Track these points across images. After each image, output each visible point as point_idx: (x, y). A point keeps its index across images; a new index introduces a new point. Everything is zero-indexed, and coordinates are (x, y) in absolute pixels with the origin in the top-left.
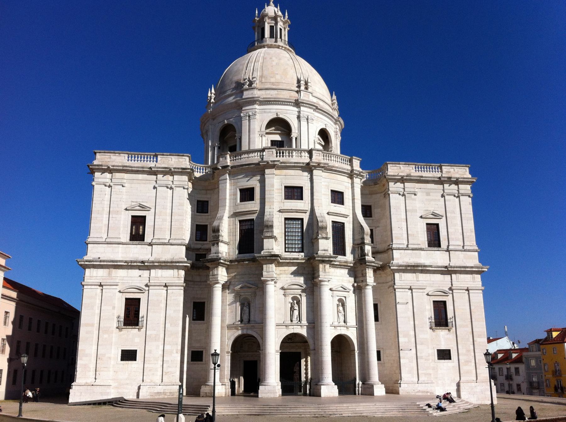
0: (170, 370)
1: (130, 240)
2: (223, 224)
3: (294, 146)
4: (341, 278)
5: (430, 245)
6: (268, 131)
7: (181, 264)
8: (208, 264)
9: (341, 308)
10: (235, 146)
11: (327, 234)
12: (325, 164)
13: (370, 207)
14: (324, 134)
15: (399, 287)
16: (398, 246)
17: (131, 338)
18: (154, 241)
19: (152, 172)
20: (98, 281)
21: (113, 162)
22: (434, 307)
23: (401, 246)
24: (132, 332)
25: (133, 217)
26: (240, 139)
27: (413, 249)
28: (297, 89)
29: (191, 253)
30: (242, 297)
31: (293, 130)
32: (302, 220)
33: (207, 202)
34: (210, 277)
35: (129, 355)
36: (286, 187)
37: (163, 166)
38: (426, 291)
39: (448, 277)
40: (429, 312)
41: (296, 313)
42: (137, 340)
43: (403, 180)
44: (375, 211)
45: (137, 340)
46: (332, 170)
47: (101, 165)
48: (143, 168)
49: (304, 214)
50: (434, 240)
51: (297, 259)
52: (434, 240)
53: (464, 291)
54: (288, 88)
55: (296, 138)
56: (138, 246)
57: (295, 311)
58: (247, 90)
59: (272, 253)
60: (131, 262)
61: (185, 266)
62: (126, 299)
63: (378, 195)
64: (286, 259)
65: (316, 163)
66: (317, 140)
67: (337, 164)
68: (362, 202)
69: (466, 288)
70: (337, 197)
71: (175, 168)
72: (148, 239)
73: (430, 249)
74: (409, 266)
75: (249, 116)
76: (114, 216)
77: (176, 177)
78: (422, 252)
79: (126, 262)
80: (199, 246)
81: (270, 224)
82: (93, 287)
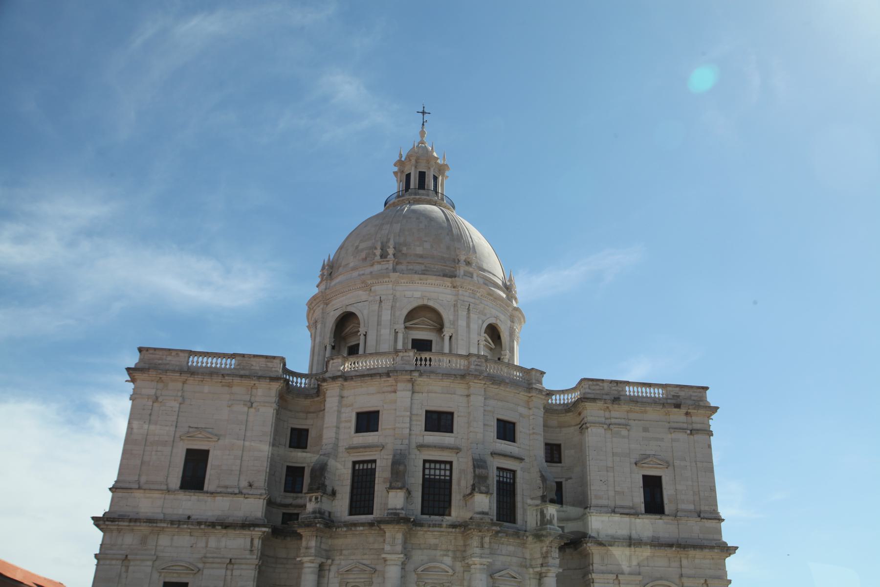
3: (447, 350)
6: (408, 324)
7: (257, 529)
8: (299, 531)
10: (358, 345)
11: (488, 487)
13: (558, 446)
14: (493, 332)
18: (219, 490)
21: (166, 364)
26: (365, 335)
32: (451, 463)
33: (307, 431)
34: (303, 550)
36: (427, 412)
44: (566, 453)
55: (451, 337)
58: (379, 263)
59: (401, 515)
61: (264, 532)
63: (572, 429)
68: (544, 439)
70: (506, 430)
72: (210, 483)
76: (159, 448)
80: (289, 501)
81: (401, 468)
82: (114, 562)
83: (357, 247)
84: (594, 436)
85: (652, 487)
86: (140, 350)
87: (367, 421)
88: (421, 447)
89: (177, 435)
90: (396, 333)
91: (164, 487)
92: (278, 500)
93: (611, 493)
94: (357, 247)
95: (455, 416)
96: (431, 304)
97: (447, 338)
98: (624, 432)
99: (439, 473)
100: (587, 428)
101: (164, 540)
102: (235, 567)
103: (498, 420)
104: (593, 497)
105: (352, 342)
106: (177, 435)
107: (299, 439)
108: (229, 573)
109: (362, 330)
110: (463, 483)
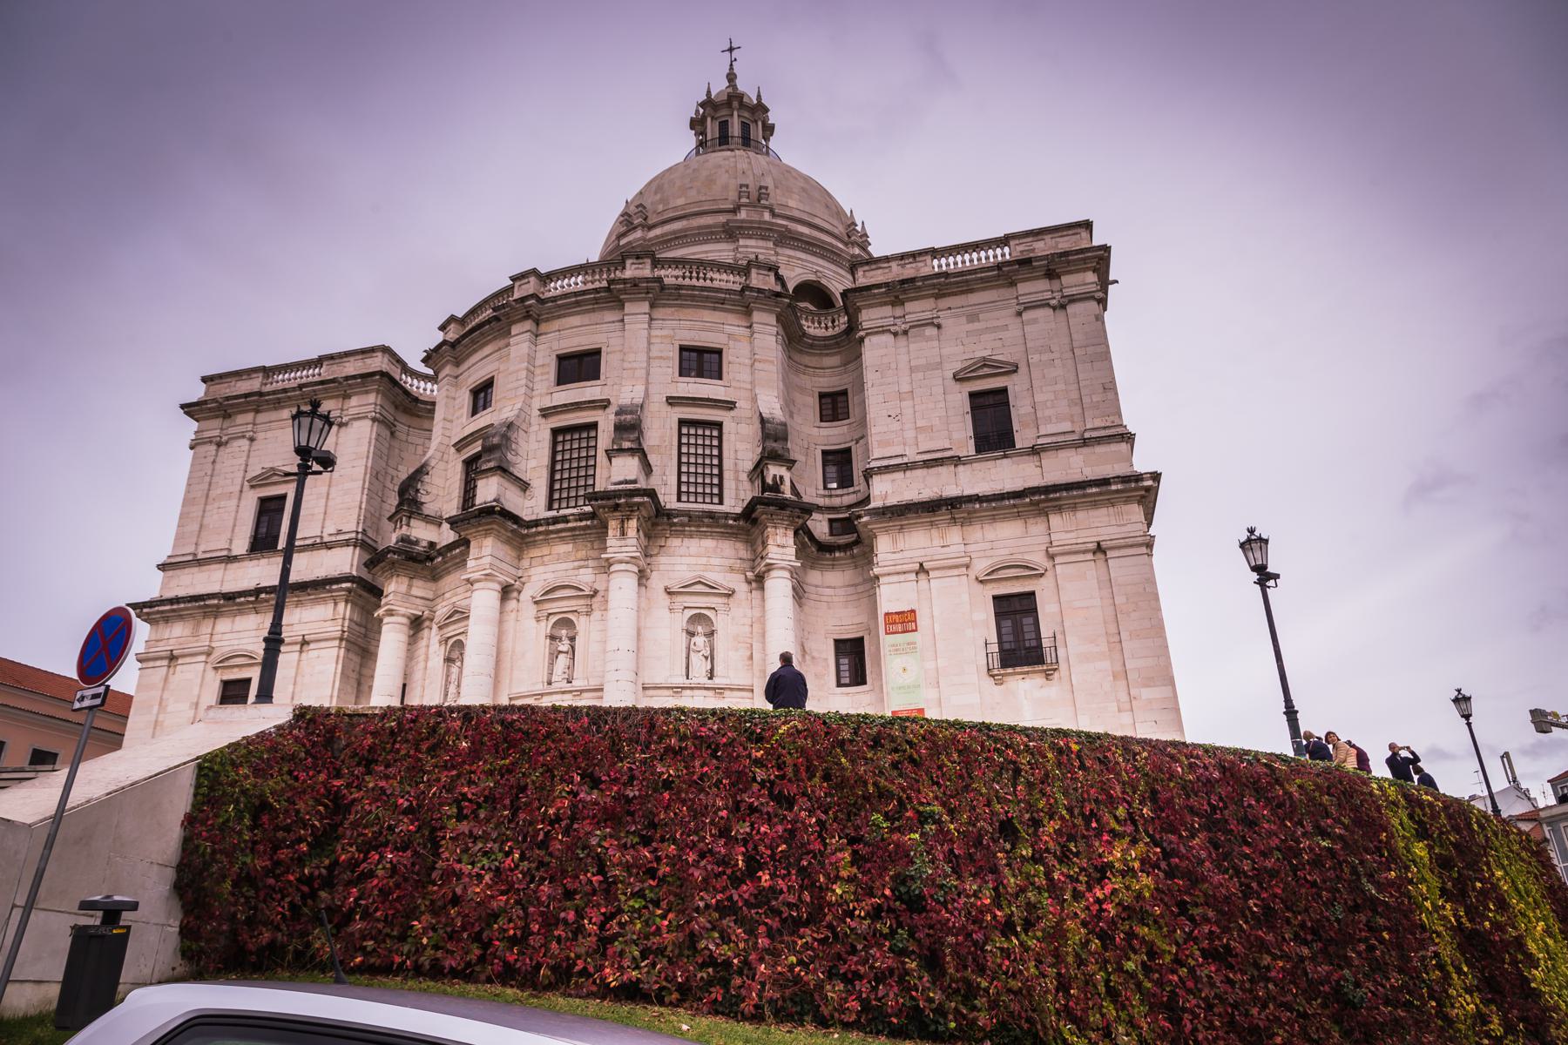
2: (426, 478)
4: (704, 560)
5: (979, 450)
9: (700, 640)
15: (886, 570)
16: (885, 463)
22: (999, 615)
27: (928, 464)
30: (451, 642)
39: (1037, 527)
40: (983, 626)
41: (562, 661)
46: (680, 297)
48: (285, 391)
49: (600, 412)
53: (1090, 556)
56: (263, 561)
57: (561, 656)
61: (349, 590)
69: (1093, 546)
70: (701, 361)
71: (347, 378)
76: (223, 504)
77: (354, 401)
78: (961, 468)
82: (158, 663)
84: (875, 350)
86: (204, 380)
88: (546, 413)
93: (910, 434)
98: (931, 331)
100: (862, 340)
101: (223, 625)
102: (312, 646)
103: (683, 349)
104: (875, 444)
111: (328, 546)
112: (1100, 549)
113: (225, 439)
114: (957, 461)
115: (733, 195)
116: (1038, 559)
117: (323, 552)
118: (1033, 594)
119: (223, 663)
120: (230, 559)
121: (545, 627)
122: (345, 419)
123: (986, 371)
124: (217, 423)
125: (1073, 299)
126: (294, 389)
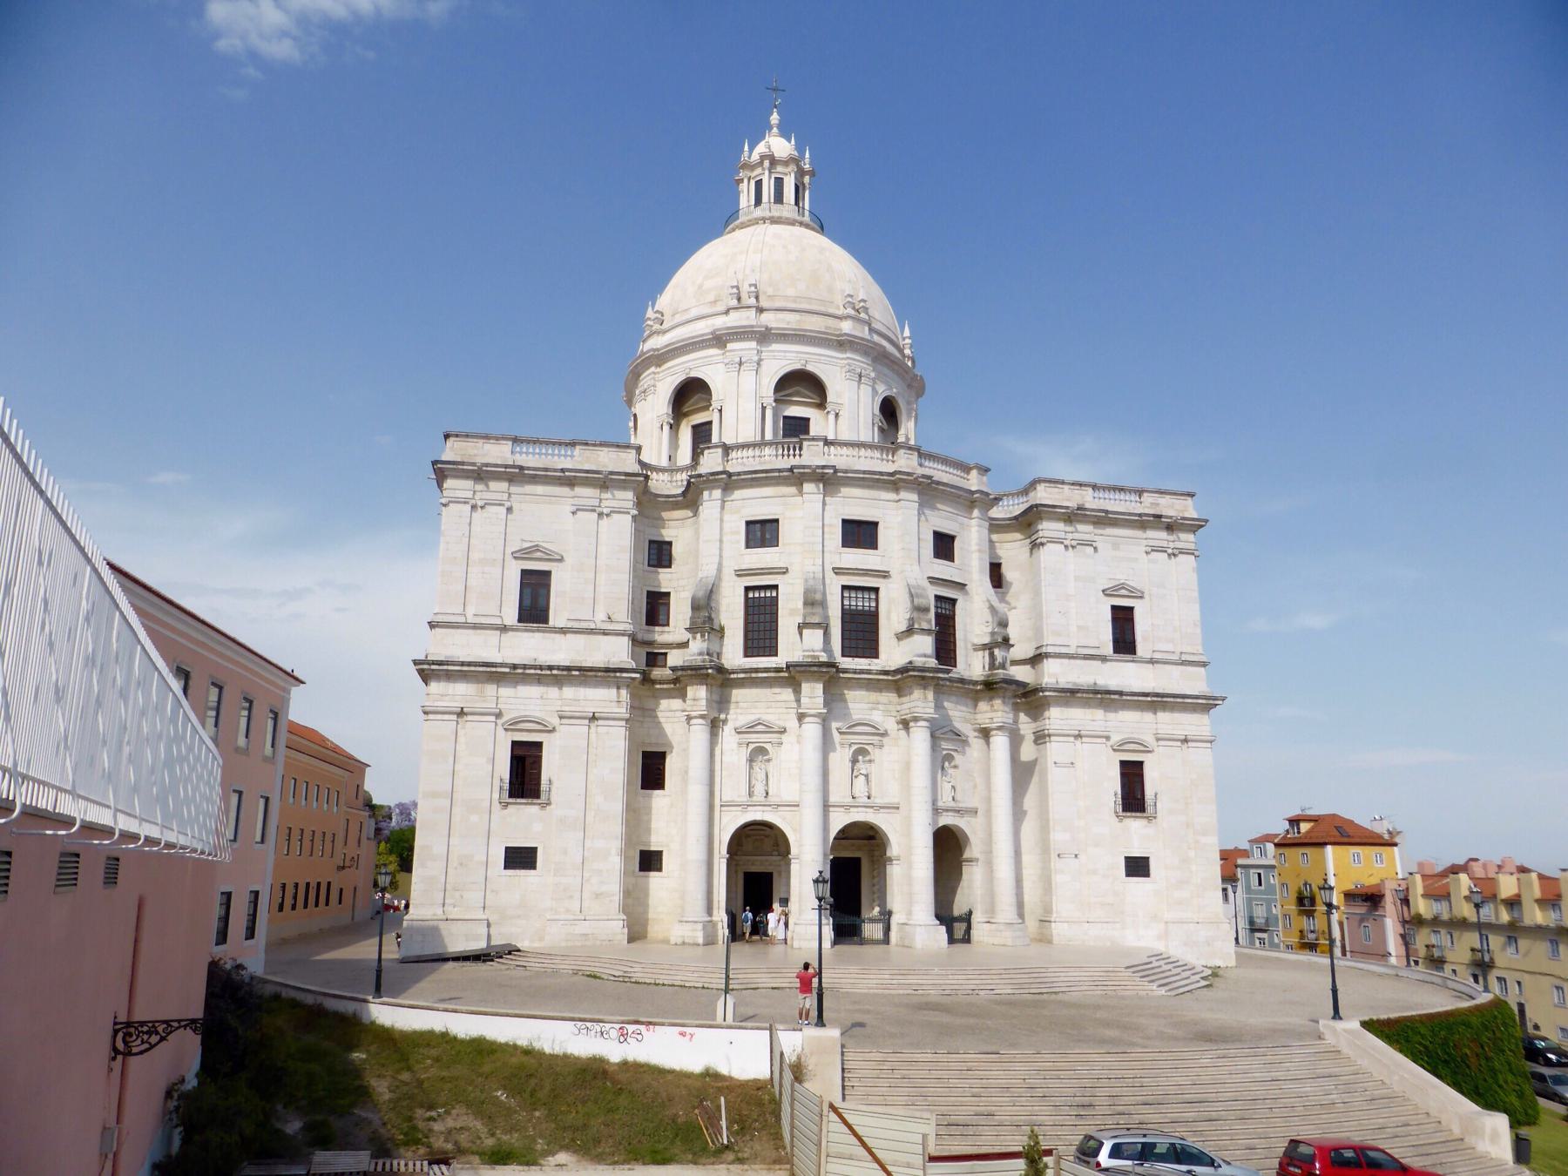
0: (604, 888)
1: (520, 620)
5: (1117, 650)
10: (710, 423)
12: (924, 476)
14: (889, 411)
16: (1057, 650)
17: (523, 823)
18: (570, 625)
19: (568, 480)
20: (456, 705)
22: (1123, 775)
23: (1063, 650)
24: (524, 812)
25: (524, 573)
28: (841, 312)
29: (637, 649)
30: (752, 746)
31: (831, 397)
32: (876, 590)
35: (521, 858)
36: (845, 522)
37: (586, 467)
38: (1112, 742)
39: (1148, 716)
40: (1113, 783)
42: (537, 827)
43: (1073, 516)
45: (537, 827)
47: (463, 463)
48: (546, 470)
50: (1124, 641)
51: (869, 672)
52: (1124, 641)
54: (823, 309)
55: (837, 415)
56: (537, 635)
60: (525, 667)
62: (514, 743)
64: (845, 671)
65: (908, 474)
66: (877, 420)
67: (945, 478)
70: (944, 545)
72: (557, 617)
73: (1118, 656)
74: (1078, 691)
75: (741, 364)
79: (515, 667)
81: (818, 597)
82: (446, 717)
83: (700, 287)
85: (1123, 620)
87: (762, 532)
88: (838, 571)
89: (509, 551)
90: (764, 408)
91: (498, 621)
92: (639, 636)
94: (700, 287)
95: (880, 527)
96: (810, 368)
97: (832, 417)
99: (861, 603)
101: (506, 692)
102: (600, 722)
105: (699, 418)
106: (509, 551)
107: (660, 554)
108: (593, 729)
109: (715, 404)
110: (894, 617)
111: (605, 633)
112: (1186, 741)
113: (480, 503)
114: (1104, 659)
115: (840, 301)
116: (1149, 739)
117: (601, 637)
118: (1141, 764)
119: (512, 726)
120: (504, 629)
121: (847, 753)
122: (606, 511)
123: (1123, 592)
124: (469, 483)
125: (1183, 552)
126: (555, 470)
